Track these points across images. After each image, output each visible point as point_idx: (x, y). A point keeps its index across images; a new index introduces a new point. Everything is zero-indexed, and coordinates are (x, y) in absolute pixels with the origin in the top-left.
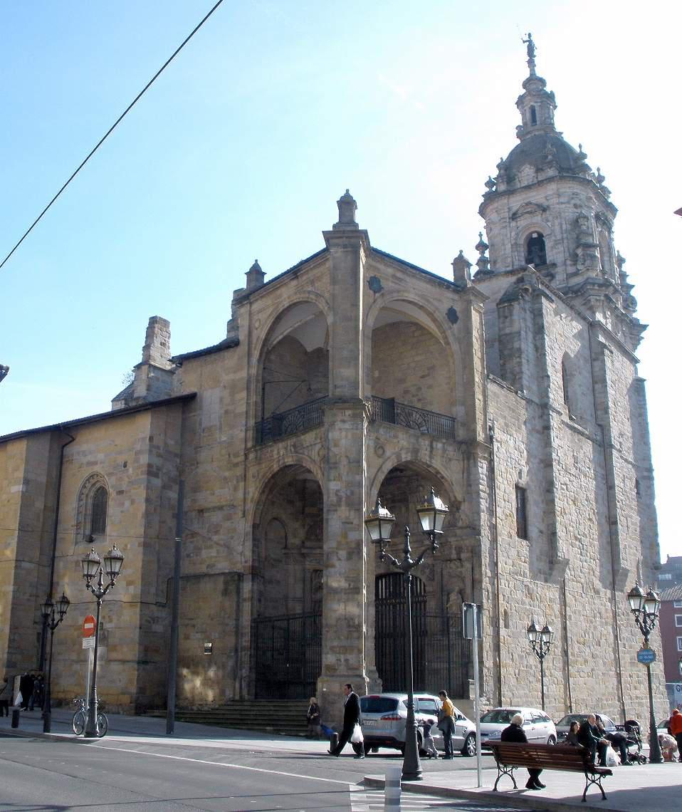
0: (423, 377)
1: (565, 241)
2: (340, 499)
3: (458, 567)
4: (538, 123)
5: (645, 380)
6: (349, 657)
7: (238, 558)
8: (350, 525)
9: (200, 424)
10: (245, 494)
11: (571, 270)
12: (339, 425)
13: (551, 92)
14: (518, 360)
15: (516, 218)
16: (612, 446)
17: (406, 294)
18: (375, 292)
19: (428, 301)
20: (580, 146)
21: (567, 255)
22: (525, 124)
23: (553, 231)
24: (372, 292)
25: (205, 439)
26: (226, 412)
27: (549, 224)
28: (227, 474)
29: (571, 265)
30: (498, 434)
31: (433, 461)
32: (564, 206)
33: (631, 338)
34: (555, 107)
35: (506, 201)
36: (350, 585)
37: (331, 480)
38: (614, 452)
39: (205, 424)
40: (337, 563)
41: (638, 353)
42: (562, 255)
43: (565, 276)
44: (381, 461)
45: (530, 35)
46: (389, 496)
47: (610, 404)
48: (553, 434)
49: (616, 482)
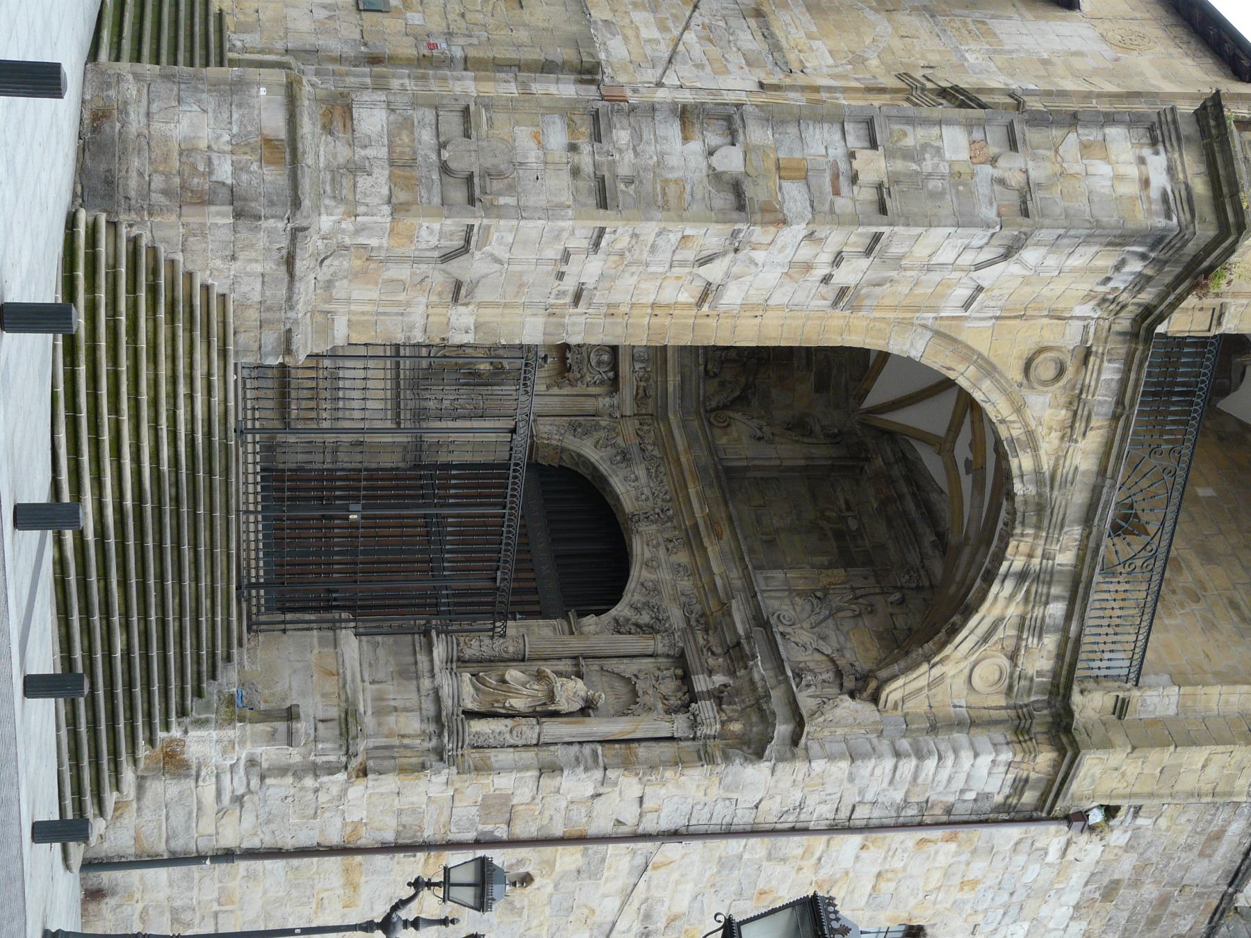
0: (1234, 605)
2: (907, 155)
3: (665, 698)
6: (381, 175)
7: (651, 75)
8: (828, 188)
9: (993, 17)
10: (830, 89)
12: (1157, 164)
25: (958, 24)
26: (1045, 63)
28: (874, 62)
30: (1089, 849)
31: (1009, 585)
36: (629, 181)
37: (970, 133)
39: (1000, 26)
40: (696, 146)
44: (1015, 373)
46: (853, 525)
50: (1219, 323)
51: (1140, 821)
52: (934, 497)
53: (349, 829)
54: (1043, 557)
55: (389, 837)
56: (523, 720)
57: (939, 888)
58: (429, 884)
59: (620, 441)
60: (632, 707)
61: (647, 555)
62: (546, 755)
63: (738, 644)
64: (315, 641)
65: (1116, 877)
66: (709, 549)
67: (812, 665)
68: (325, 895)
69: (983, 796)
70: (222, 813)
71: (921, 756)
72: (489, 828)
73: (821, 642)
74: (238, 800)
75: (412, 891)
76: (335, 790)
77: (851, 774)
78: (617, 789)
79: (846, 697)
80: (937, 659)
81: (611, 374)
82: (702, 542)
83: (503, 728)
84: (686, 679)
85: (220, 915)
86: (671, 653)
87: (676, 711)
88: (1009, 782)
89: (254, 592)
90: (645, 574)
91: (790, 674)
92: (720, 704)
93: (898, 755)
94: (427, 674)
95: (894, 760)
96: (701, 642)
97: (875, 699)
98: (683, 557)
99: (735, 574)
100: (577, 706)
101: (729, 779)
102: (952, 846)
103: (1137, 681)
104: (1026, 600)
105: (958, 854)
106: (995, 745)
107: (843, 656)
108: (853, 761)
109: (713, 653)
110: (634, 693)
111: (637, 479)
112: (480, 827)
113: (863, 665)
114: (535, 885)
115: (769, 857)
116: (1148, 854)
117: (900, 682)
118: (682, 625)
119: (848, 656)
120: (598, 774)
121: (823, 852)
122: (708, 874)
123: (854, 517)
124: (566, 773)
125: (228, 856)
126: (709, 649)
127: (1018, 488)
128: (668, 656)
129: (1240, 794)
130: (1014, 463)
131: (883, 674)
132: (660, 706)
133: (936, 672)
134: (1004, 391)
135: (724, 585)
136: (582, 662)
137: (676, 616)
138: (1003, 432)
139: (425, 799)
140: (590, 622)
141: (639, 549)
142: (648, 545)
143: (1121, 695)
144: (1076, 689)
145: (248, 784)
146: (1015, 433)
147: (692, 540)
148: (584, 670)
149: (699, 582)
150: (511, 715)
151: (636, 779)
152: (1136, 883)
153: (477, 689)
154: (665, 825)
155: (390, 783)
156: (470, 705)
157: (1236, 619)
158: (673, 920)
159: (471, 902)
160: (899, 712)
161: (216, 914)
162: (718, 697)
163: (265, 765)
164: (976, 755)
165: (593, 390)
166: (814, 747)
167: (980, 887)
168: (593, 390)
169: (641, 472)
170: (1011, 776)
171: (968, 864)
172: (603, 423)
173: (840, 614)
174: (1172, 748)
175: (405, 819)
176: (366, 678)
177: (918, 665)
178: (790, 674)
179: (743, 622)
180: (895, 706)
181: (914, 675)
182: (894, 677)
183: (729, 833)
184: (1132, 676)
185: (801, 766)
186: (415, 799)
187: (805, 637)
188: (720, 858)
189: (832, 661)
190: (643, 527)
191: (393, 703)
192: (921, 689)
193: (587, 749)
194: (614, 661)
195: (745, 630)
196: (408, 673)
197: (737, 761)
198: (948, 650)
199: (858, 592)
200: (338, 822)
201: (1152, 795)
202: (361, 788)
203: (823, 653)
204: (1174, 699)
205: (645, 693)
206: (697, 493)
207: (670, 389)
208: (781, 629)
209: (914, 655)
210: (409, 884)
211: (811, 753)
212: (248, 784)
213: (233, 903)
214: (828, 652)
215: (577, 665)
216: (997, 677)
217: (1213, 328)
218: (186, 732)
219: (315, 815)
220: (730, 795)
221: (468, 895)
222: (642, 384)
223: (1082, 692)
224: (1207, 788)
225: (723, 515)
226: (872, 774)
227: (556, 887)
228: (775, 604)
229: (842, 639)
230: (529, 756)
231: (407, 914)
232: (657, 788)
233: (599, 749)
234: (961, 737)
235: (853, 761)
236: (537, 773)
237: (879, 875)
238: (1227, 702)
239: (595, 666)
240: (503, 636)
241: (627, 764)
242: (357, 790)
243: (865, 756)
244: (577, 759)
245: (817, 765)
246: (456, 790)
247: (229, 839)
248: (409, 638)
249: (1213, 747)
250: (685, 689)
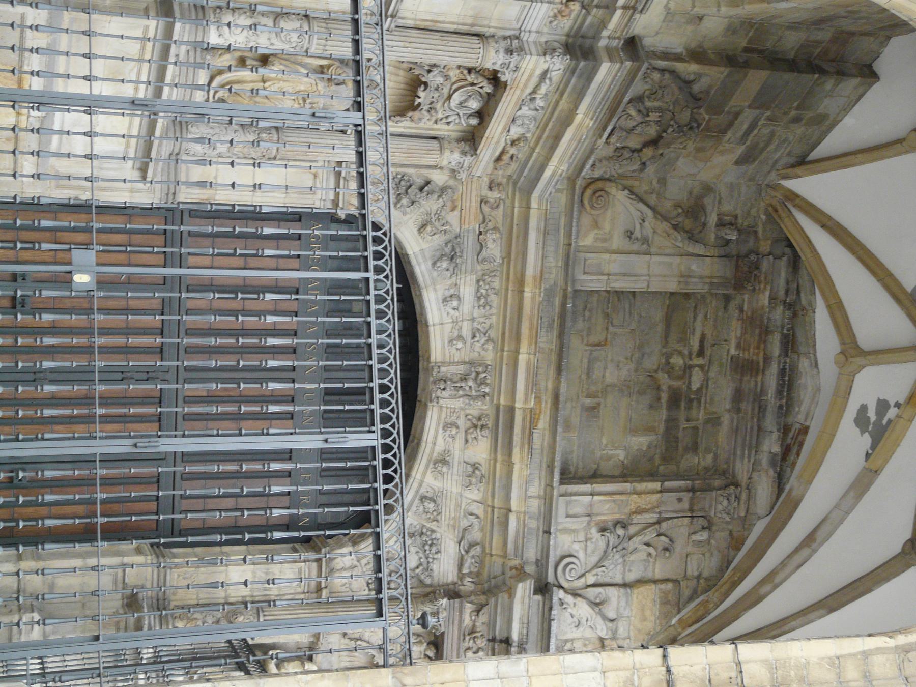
52: (804, 364)
61: (440, 446)
66: (516, 468)
82: (510, 455)
90: (429, 479)
123: (701, 367)
135: (517, 532)
149: (490, 499)
195: (520, 633)
206: (528, 363)
207: (547, 173)
225: (550, 386)
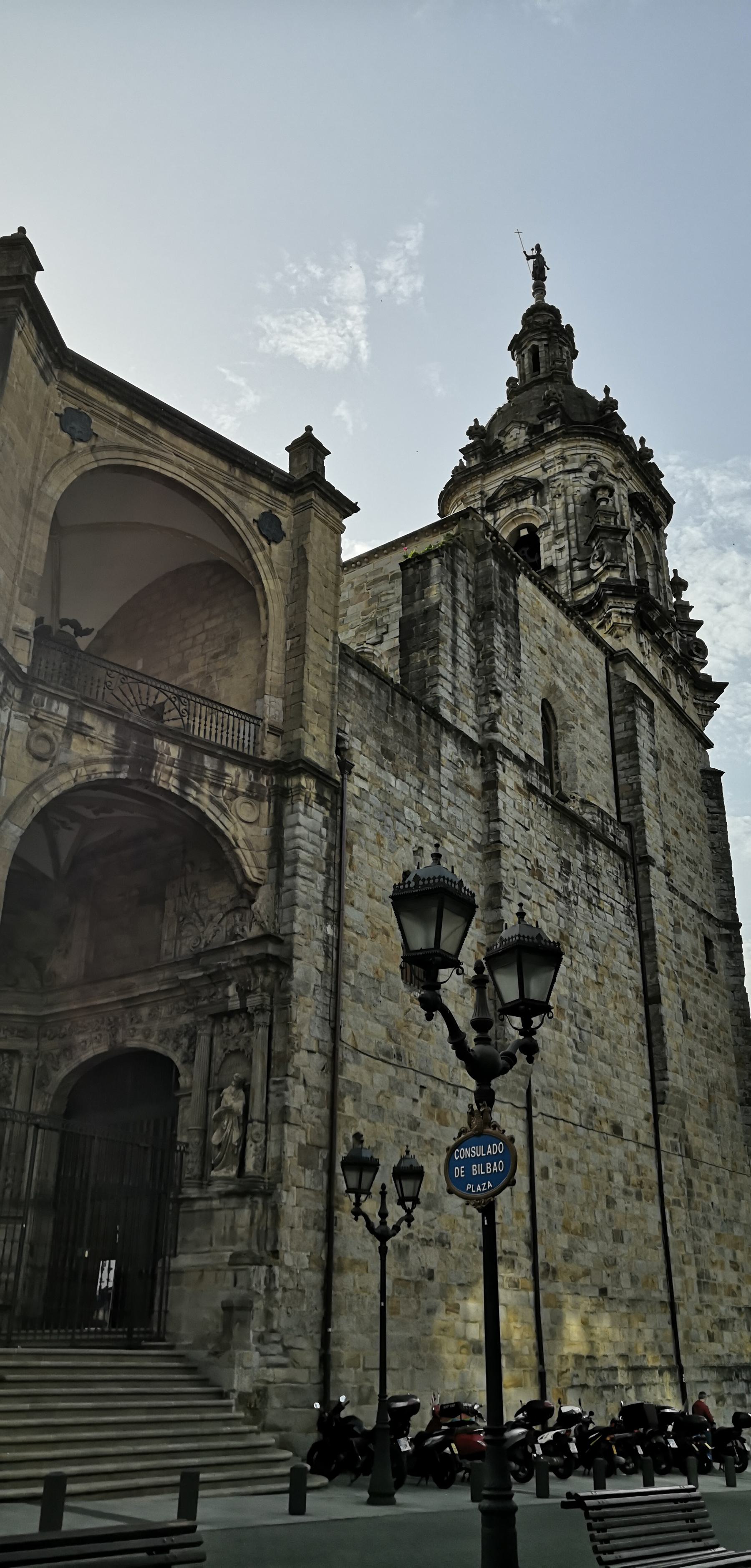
0: (216, 656)
1: (572, 531)
4: (542, 370)
5: (722, 773)
11: (580, 575)
13: (568, 326)
14: (432, 654)
15: (495, 505)
16: (648, 861)
17: (157, 462)
18: (74, 439)
19: (213, 488)
20: (607, 390)
21: (574, 552)
22: (522, 375)
23: (553, 517)
24: (65, 436)
27: (547, 507)
29: (581, 568)
30: (362, 763)
32: (572, 476)
33: (695, 704)
34: (574, 354)
35: (479, 482)
38: (653, 871)
41: (708, 732)
42: (566, 552)
43: (570, 587)
45: (538, 248)
47: (645, 788)
48: (500, 794)
49: (658, 926)
50: (27, 633)
51: (347, 731)
53: (314, 1266)
54: (172, 766)
55: (321, 1236)
56: (249, 1133)
57: (381, 859)
58: (358, 1203)
59: (56, 1052)
60: (246, 1053)
61: (139, 1037)
62: (274, 1118)
63: (210, 976)
64: (176, 1288)
65: (379, 750)
67: (229, 927)
68: (358, 1286)
69: (325, 824)
70: (295, 1364)
71: (297, 860)
72: (320, 1162)
73: (215, 919)
74: (287, 1350)
75: (361, 1218)
76: (286, 1276)
77: (304, 907)
78: (302, 1068)
79: (253, 906)
80: (234, 843)
81: (5, 1055)
83: (253, 1147)
84: (231, 1015)
85: (366, 1366)
86: (211, 1024)
87: (251, 1023)
88: (318, 806)
89: (135, 1336)
91: (234, 942)
92: (249, 992)
93: (294, 875)
94: (209, 1202)
95: (298, 878)
96: (205, 1002)
97: (257, 886)
98: (144, 1012)
99: (161, 976)
100: (242, 1093)
101: (301, 989)
102: (355, 847)
103: (259, 719)
104: (200, 781)
105: (360, 845)
106: (292, 812)
107: (225, 905)
108: (297, 905)
109: (214, 994)
110: (237, 1052)
111: (85, 1041)
112: (320, 1168)
113: (232, 892)
114: (362, 1132)
115: (354, 967)
116: (367, 728)
117: (247, 868)
118: (192, 1015)
119: (225, 902)
120: (290, 1081)
121: (353, 931)
122: (362, 1010)
124: (287, 1103)
125: (325, 1361)
126: (211, 997)
127: (123, 776)
128: (213, 1026)
129: (334, 669)
130: (105, 776)
131: (240, 878)
132: (247, 1034)
133: (242, 844)
134: (55, 776)
136: (211, 1088)
137: (185, 1019)
138: (82, 780)
139: (297, 1208)
140: (184, 1081)
141: (134, 1043)
142: (133, 1036)
143: (267, 730)
144: (261, 757)
145: (276, 1342)
146: (84, 773)
147: (132, 1004)
148: (216, 1087)
150: (243, 1141)
151: (296, 1056)
152: (385, 738)
153: (223, 1167)
154: (327, 1037)
155: (284, 1234)
156: (233, 1173)
157: (225, 656)
158: (391, 1037)
159: (371, 1175)
160: (266, 871)
161: (366, 1369)
162: (244, 993)
163: (263, 1329)
164: (299, 824)
165: (15, 1070)
166: (284, 929)
167: (382, 832)
168: (15, 1070)
169: (80, 1038)
170: (314, 804)
171: (367, 839)
172: (41, 1064)
173: (197, 906)
174: (304, 704)
175: (310, 1224)
176: (207, 1249)
177: (236, 856)
178: (234, 942)
179: (195, 972)
180: (262, 873)
181: (243, 859)
182: (243, 872)
183: (335, 994)
184: (255, 722)
185: (297, 939)
186: (296, 1215)
187: (210, 930)
188: (353, 1001)
189: (228, 913)
190: (119, 1038)
191: (228, 1230)
192: (252, 855)
193: (272, 1088)
194: (213, 1064)
196: (208, 1215)
197: (290, 983)
198: (229, 835)
199: (183, 891)
200: (308, 1274)
201: (331, 721)
202: (286, 1256)
203: (222, 919)
204: (273, 699)
205: (237, 1044)
208: (202, 946)
209: (230, 858)
210: (356, 1219)
211: (288, 932)
212: (276, 1342)
213: (358, 1356)
214: (221, 915)
215: (213, 1091)
216: (249, 806)
217: (29, 637)
218: (234, 1391)
219: (303, 1291)
220: (312, 990)
221: (366, 1176)
222: (16, 1032)
223: (263, 754)
224: (329, 687)
226: (305, 893)
227: (364, 1117)
228: (184, 950)
229: (213, 905)
230: (273, 1130)
231: (376, 1220)
232: (303, 1041)
233: (273, 1079)
234: (287, 833)
235: (297, 905)
236: (286, 1126)
237: (370, 896)
238: (277, 668)
239: (214, 1079)
240: (187, 1145)
241: (285, 1059)
242: (288, 1260)
243: (294, 897)
244: (278, 1095)
245: (297, 928)
246: (293, 1185)
247: (311, 1358)
248: (181, 1215)
249: (305, 680)
250: (237, 1016)
